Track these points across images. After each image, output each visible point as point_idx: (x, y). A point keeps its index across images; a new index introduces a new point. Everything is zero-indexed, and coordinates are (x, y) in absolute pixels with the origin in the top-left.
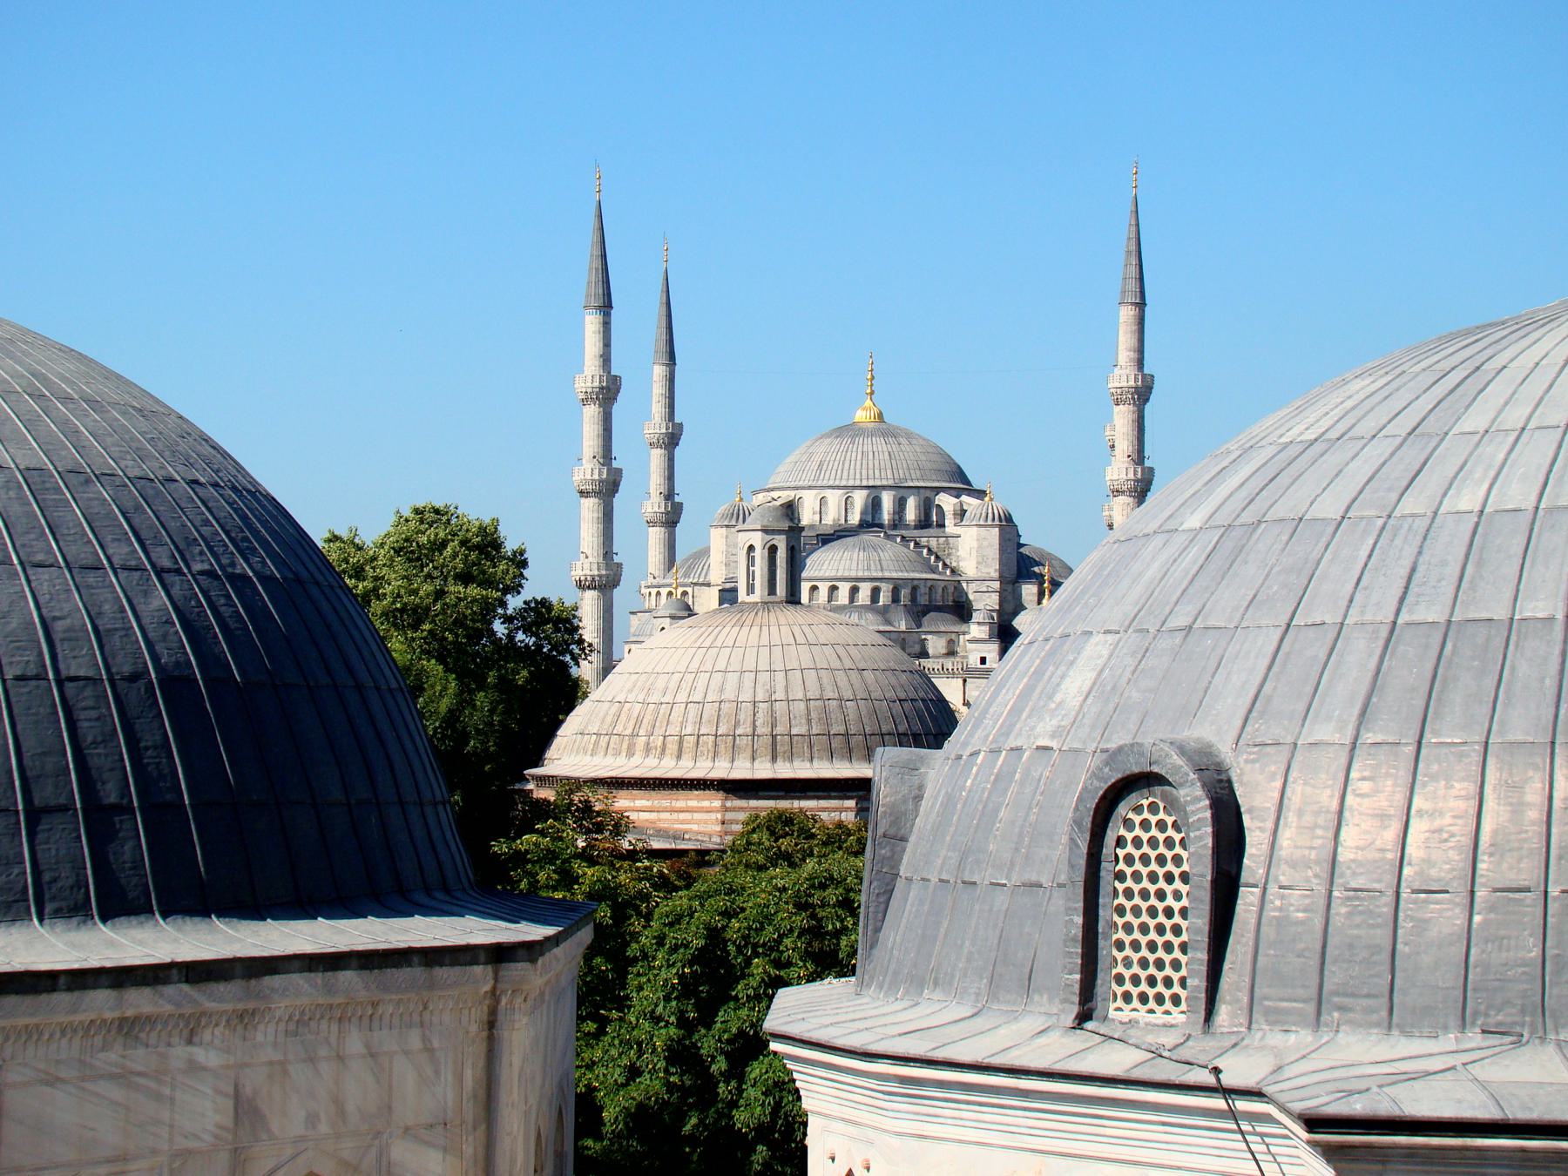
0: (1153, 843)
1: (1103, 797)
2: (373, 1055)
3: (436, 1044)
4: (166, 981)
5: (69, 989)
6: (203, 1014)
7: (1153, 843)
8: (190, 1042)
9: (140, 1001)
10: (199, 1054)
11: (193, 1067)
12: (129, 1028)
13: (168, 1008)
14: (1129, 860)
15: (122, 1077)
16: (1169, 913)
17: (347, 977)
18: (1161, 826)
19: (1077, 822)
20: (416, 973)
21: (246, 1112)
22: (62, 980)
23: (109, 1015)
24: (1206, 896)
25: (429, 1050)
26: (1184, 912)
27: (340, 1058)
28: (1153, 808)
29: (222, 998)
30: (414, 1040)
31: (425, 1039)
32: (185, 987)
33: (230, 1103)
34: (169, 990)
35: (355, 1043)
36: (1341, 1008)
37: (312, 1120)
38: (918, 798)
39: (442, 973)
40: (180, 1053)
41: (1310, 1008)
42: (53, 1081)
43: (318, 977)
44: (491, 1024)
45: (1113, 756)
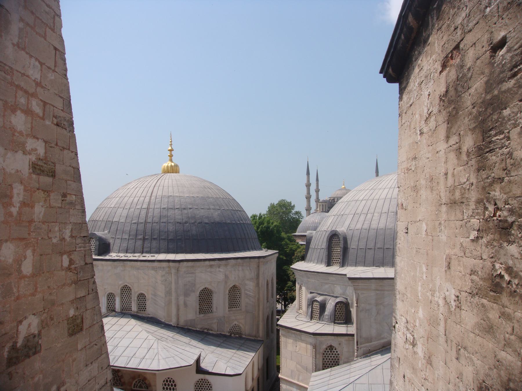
0: (336, 243)
1: (330, 237)
2: (243, 270)
3: (251, 269)
4: (216, 260)
5: (203, 261)
6: (220, 264)
7: (336, 243)
8: (219, 268)
9: (212, 263)
10: (220, 269)
11: (220, 271)
12: (211, 266)
13: (216, 264)
14: (333, 245)
15: (211, 272)
16: (338, 252)
17: (239, 260)
18: (337, 240)
19: (327, 240)
20: (248, 260)
21: (226, 277)
22: (202, 260)
23: (209, 264)
24: (342, 249)
25: (250, 269)
26: (340, 252)
27: (238, 270)
28: (336, 238)
29: (223, 262)
30: (248, 268)
31: (250, 268)
32: (218, 261)
33: (224, 276)
34: (216, 261)
35: (240, 268)
36: (358, 264)
37: (235, 278)
38: (312, 237)
39: (252, 260)
40: (218, 269)
41: (355, 264)
42: (202, 272)
43: (235, 260)
44: (258, 266)
45: (332, 231)
